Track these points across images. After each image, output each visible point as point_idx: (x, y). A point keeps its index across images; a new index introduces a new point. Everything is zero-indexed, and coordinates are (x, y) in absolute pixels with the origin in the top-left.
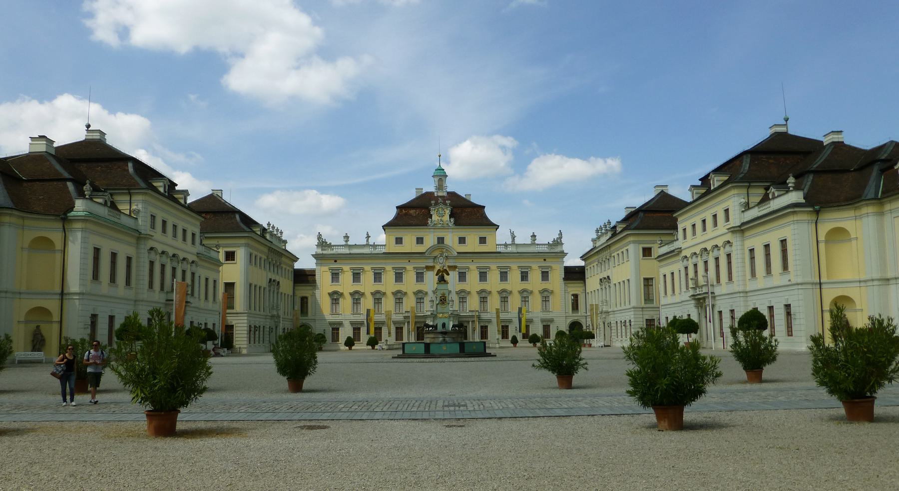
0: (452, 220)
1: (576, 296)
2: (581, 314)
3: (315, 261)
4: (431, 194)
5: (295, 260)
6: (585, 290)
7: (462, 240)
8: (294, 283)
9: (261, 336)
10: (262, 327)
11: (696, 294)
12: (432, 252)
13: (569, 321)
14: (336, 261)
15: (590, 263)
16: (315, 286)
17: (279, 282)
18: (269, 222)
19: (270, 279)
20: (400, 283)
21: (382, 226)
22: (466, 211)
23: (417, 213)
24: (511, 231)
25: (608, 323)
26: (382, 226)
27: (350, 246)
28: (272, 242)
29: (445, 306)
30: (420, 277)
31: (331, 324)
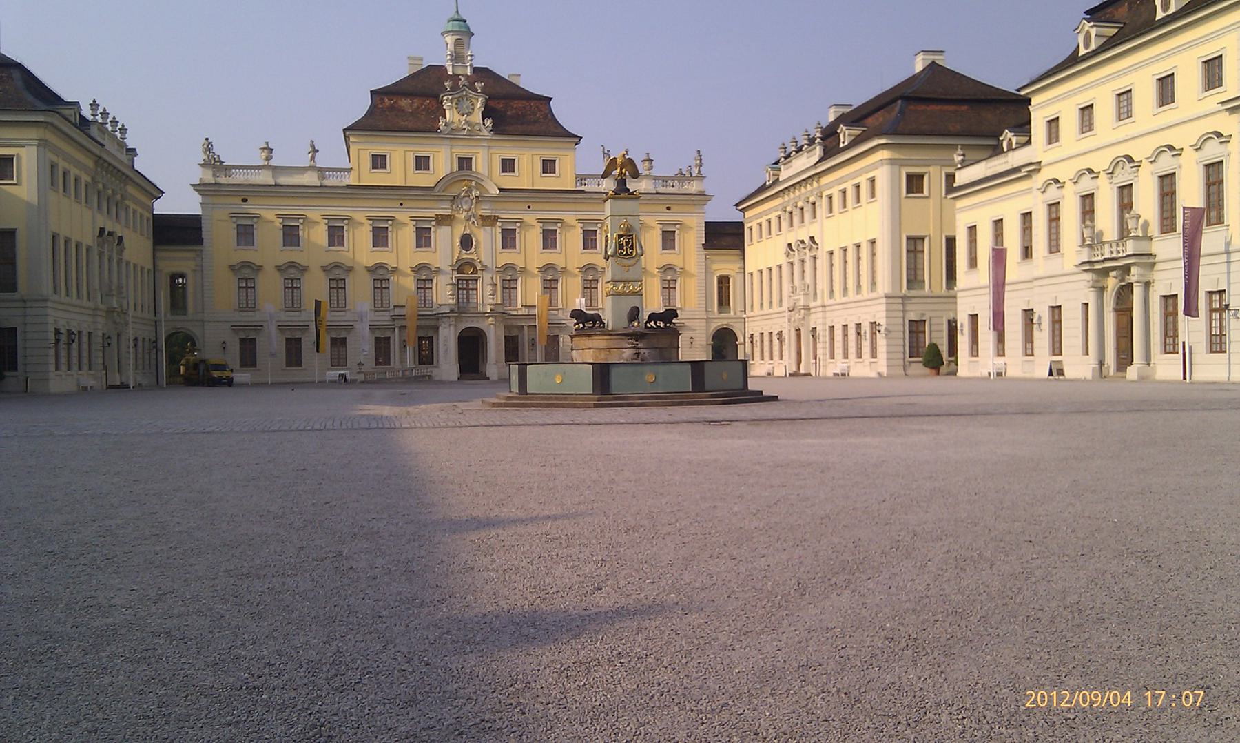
0: (489, 122)
1: (724, 282)
2: (735, 314)
3: (199, 198)
4: (442, 69)
5: (157, 195)
6: (744, 269)
7: (508, 165)
8: (154, 246)
9: (85, 354)
10: (85, 333)
11: (1100, 258)
12: (446, 188)
13: (714, 326)
14: (245, 200)
15: (759, 215)
16: (202, 250)
17: (121, 239)
18: (94, 101)
19: (102, 230)
20: (382, 249)
21: (344, 130)
22: (515, 106)
23: (416, 105)
24: (604, 149)
25: (778, 334)
26: (344, 130)
27: (276, 170)
28: (102, 145)
29: (632, 261)
30: (423, 237)
31: (235, 329)
